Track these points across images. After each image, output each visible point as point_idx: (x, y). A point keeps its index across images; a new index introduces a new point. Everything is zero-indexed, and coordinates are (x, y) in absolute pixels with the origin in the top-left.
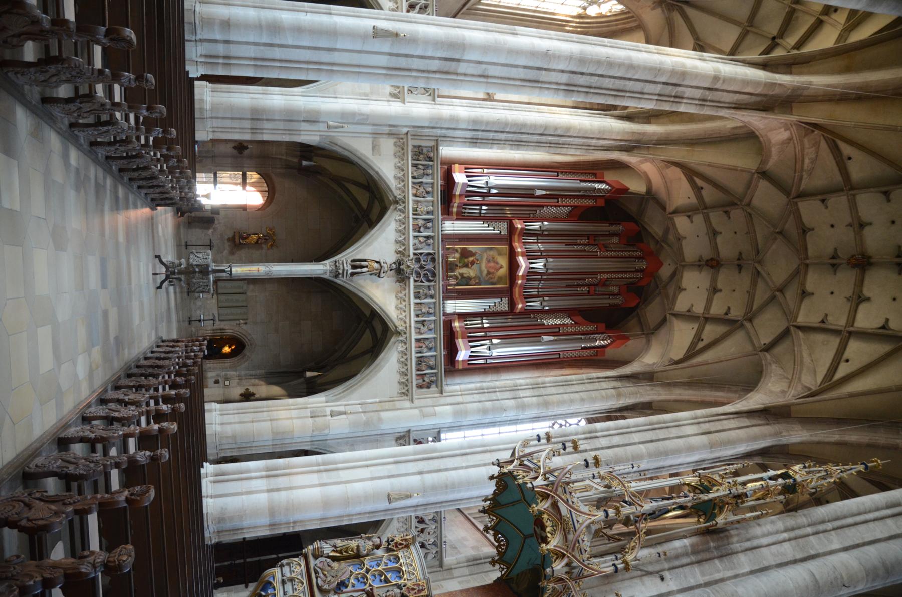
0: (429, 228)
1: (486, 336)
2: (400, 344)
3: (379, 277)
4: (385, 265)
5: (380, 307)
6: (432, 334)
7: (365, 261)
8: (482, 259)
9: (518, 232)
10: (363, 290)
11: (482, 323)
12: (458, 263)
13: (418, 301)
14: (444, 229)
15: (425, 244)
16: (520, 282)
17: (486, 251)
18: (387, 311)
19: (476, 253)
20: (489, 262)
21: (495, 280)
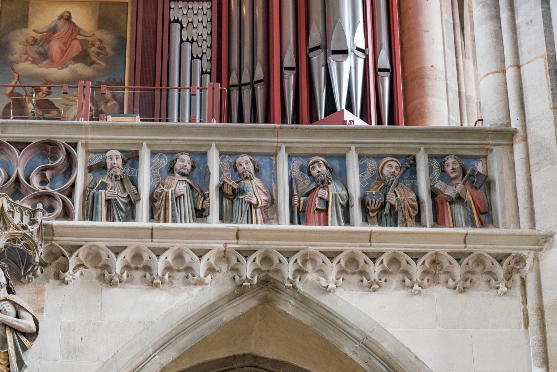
2: (311, 276)
3: (32, 336)
6: (274, 167)
8: (35, 77)
13: (143, 207)
17: (11, 64)
20: (44, 56)
21: (107, 38)
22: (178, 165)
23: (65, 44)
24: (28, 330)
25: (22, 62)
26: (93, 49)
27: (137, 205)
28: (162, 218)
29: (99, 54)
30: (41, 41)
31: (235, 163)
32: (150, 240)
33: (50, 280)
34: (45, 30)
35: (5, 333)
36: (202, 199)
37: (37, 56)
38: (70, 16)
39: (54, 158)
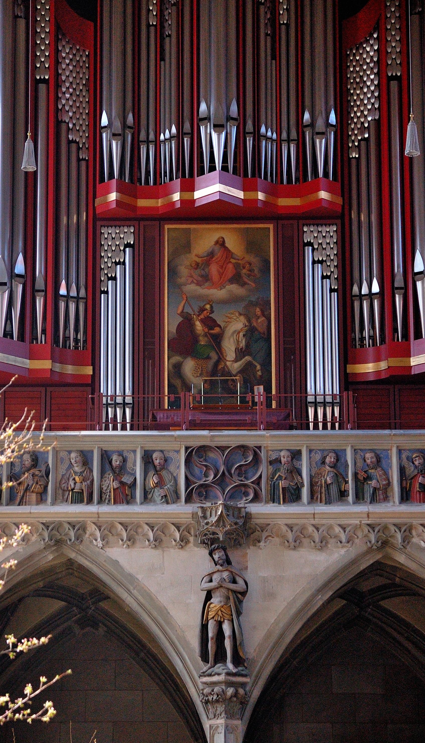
0: (125, 460)
1: (406, 288)
3: (244, 594)
4: (216, 577)
5: (320, 590)
6: (389, 458)
7: (204, 628)
8: (199, 297)
9: (127, 199)
10: (277, 632)
11: (371, 295)
12: (211, 364)
14: (119, 400)
15: (164, 473)
16: (261, 196)
17: (179, 286)
18: (330, 573)
19: (182, 314)
22: (328, 460)
23: (222, 267)
24: (242, 591)
25: (188, 284)
26: (244, 271)
27: (302, 489)
28: (319, 500)
29: (249, 276)
30: (202, 264)
31: (365, 457)
32: (313, 520)
33: (251, 547)
34: (205, 255)
35: (228, 593)
36: (344, 483)
37: (200, 279)
38: (224, 241)
39: (246, 457)
